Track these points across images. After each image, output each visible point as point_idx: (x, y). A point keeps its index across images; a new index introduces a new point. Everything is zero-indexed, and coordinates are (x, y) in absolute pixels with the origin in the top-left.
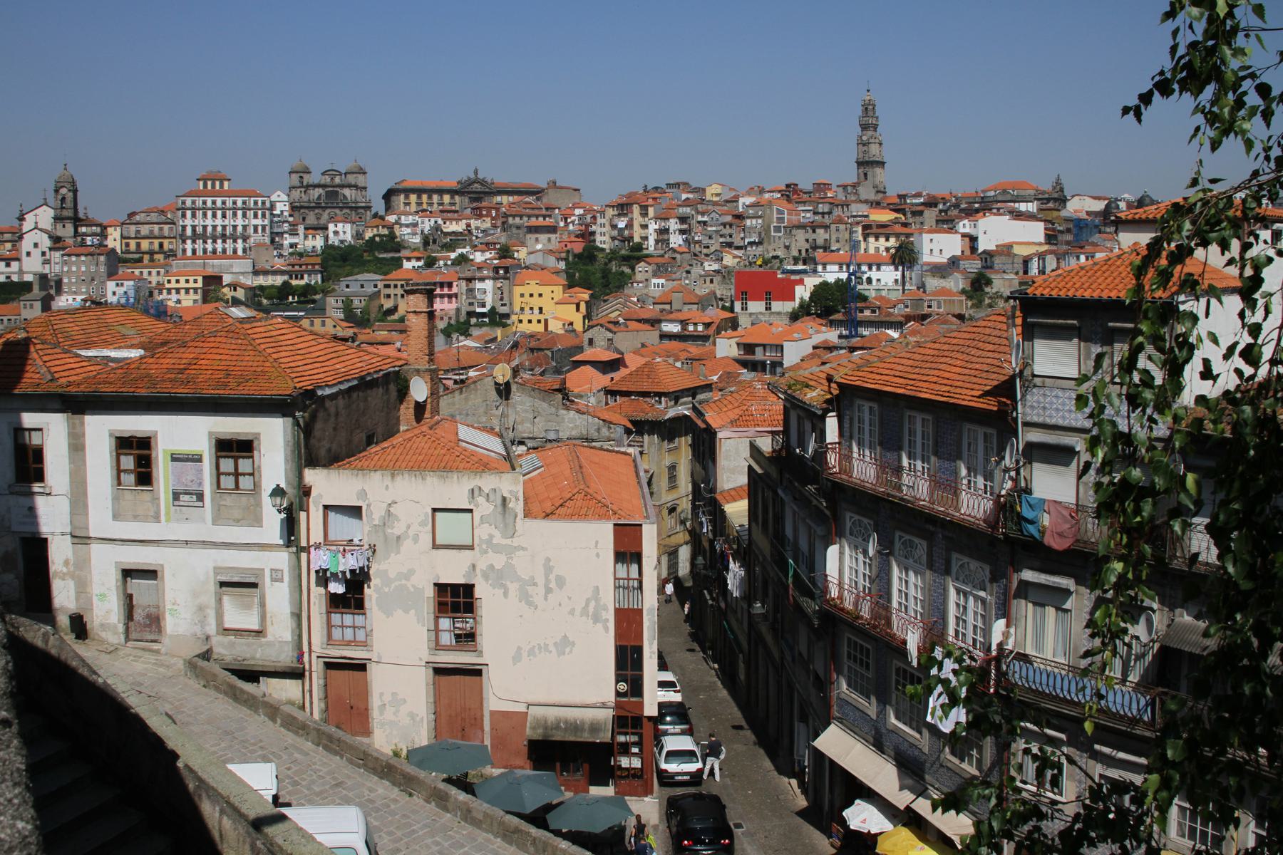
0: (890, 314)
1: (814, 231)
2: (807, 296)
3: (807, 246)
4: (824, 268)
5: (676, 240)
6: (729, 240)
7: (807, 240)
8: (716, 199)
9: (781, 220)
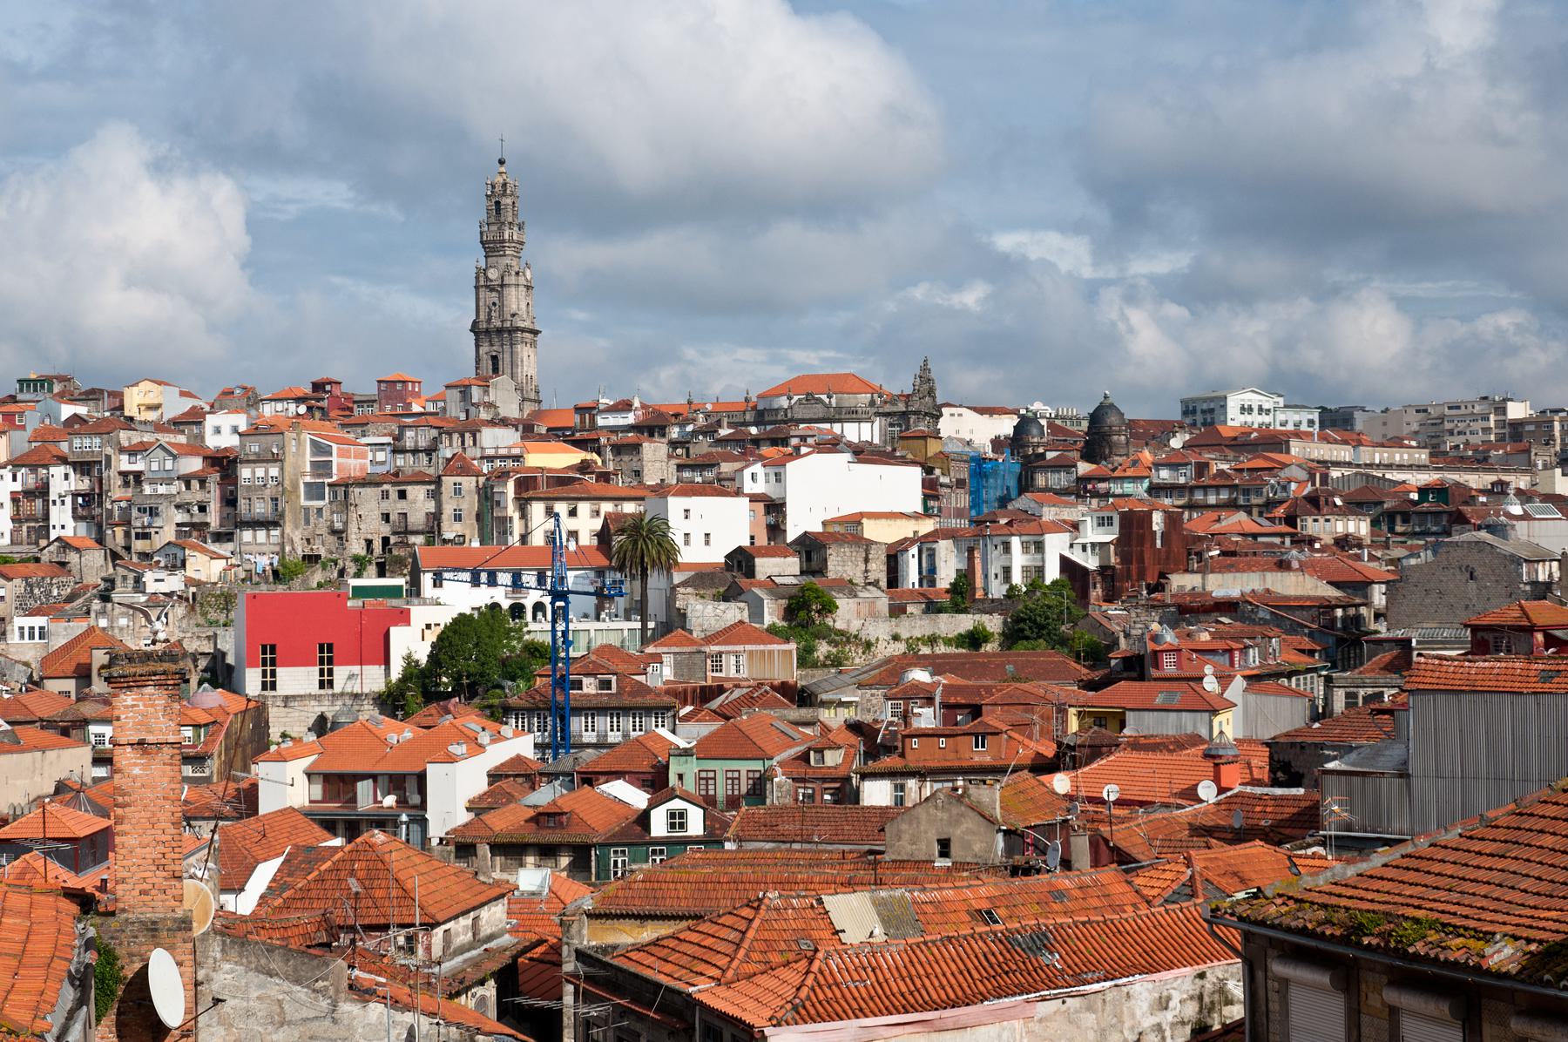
0: (643, 689)
1: (402, 495)
2: (422, 654)
3: (386, 530)
4: (438, 582)
5: (63, 521)
6: (198, 518)
7: (386, 517)
8: (152, 416)
9: (322, 468)
